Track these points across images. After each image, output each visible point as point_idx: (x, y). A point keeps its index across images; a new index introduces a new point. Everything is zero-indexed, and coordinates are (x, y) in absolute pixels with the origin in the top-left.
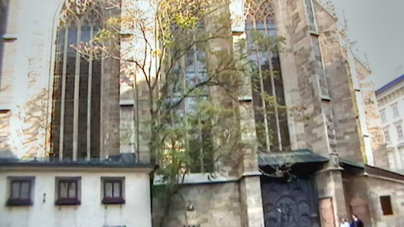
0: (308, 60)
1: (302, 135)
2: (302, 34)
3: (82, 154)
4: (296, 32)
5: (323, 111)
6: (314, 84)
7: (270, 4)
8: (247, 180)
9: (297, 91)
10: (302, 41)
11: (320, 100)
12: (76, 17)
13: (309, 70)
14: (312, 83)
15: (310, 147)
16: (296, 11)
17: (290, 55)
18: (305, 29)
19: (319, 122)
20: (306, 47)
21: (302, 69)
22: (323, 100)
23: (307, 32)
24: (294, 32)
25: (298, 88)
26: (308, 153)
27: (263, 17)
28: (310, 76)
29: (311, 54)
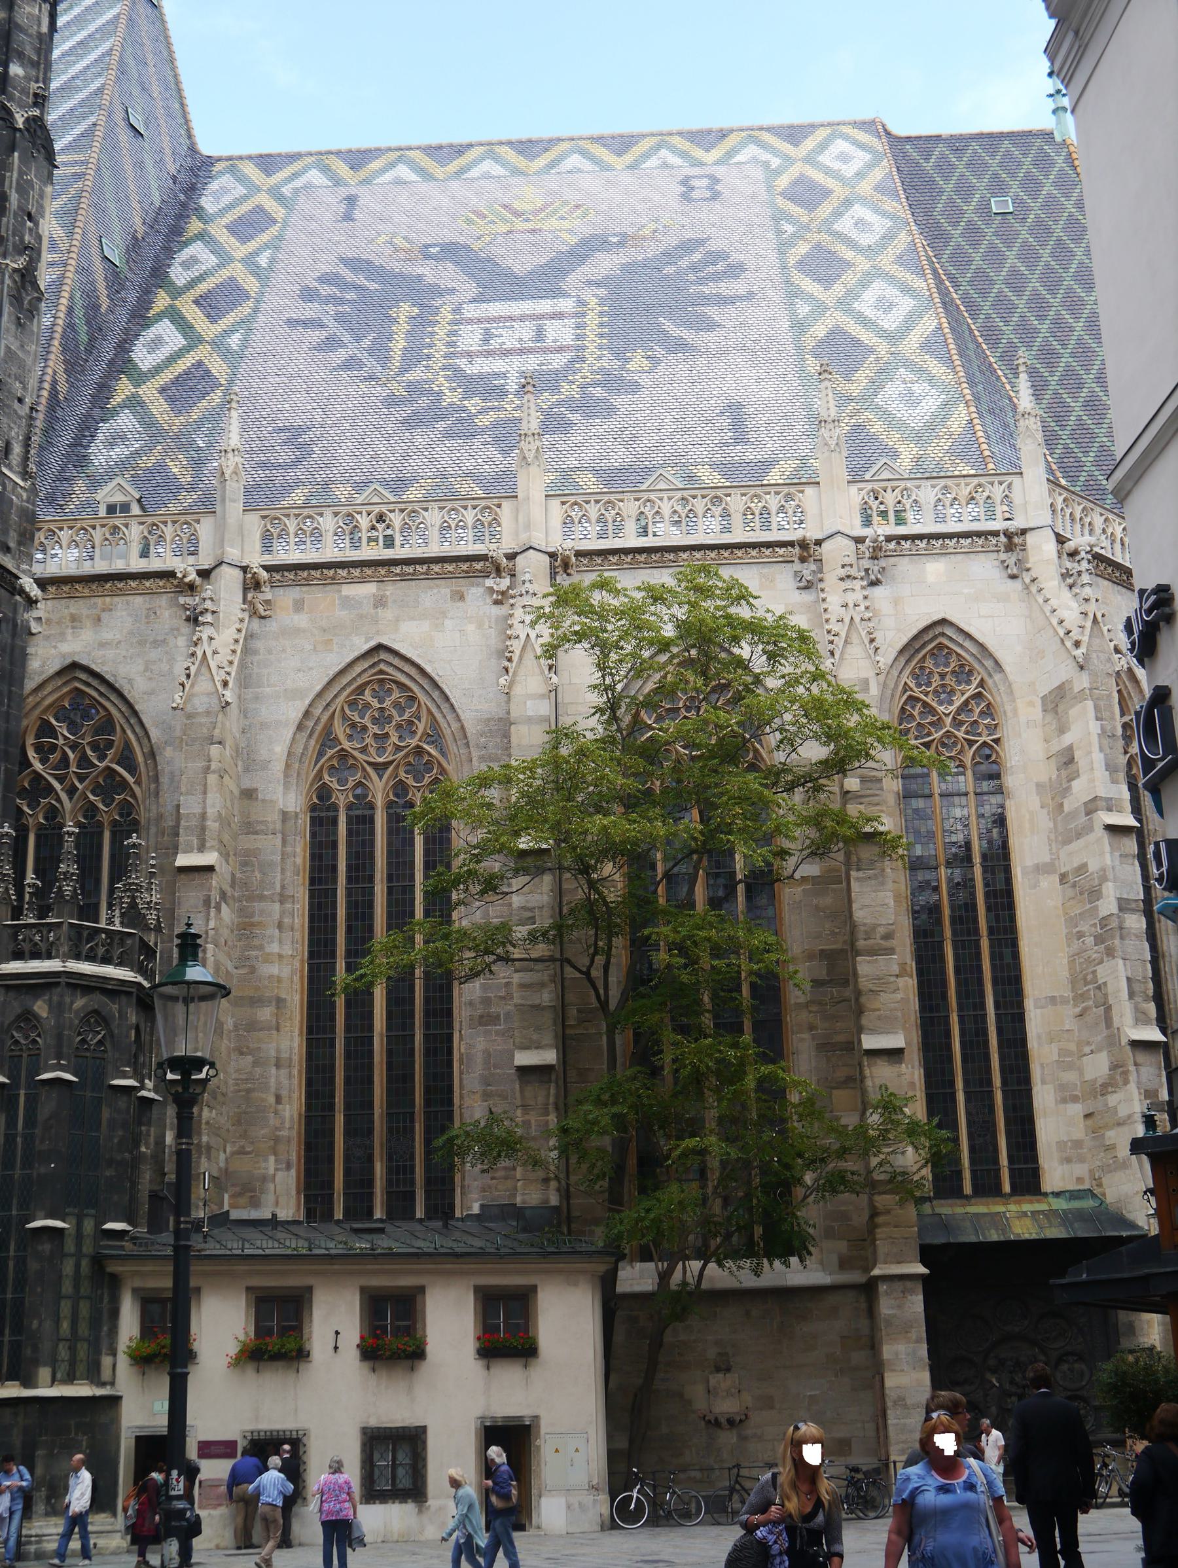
0: (1096, 908)
1: (1078, 1144)
2: (1083, 819)
3: (400, 1206)
4: (1066, 809)
5: (1133, 1077)
6: (1110, 989)
7: (989, 705)
8: (883, 1288)
9: (1064, 1001)
10: (1081, 842)
11: (1124, 1041)
12: (368, 769)
13: (1099, 940)
14: (1105, 983)
15: (1100, 1185)
16: (1068, 739)
17: (1049, 883)
18: (1091, 807)
19: (1123, 1112)
20: (1093, 866)
21: (1080, 935)
22: (1136, 1044)
23: (1095, 816)
24: (1062, 805)
25: (1068, 993)
26: (1089, 1204)
27: (961, 752)
28: (1101, 962)
29: (1104, 891)
